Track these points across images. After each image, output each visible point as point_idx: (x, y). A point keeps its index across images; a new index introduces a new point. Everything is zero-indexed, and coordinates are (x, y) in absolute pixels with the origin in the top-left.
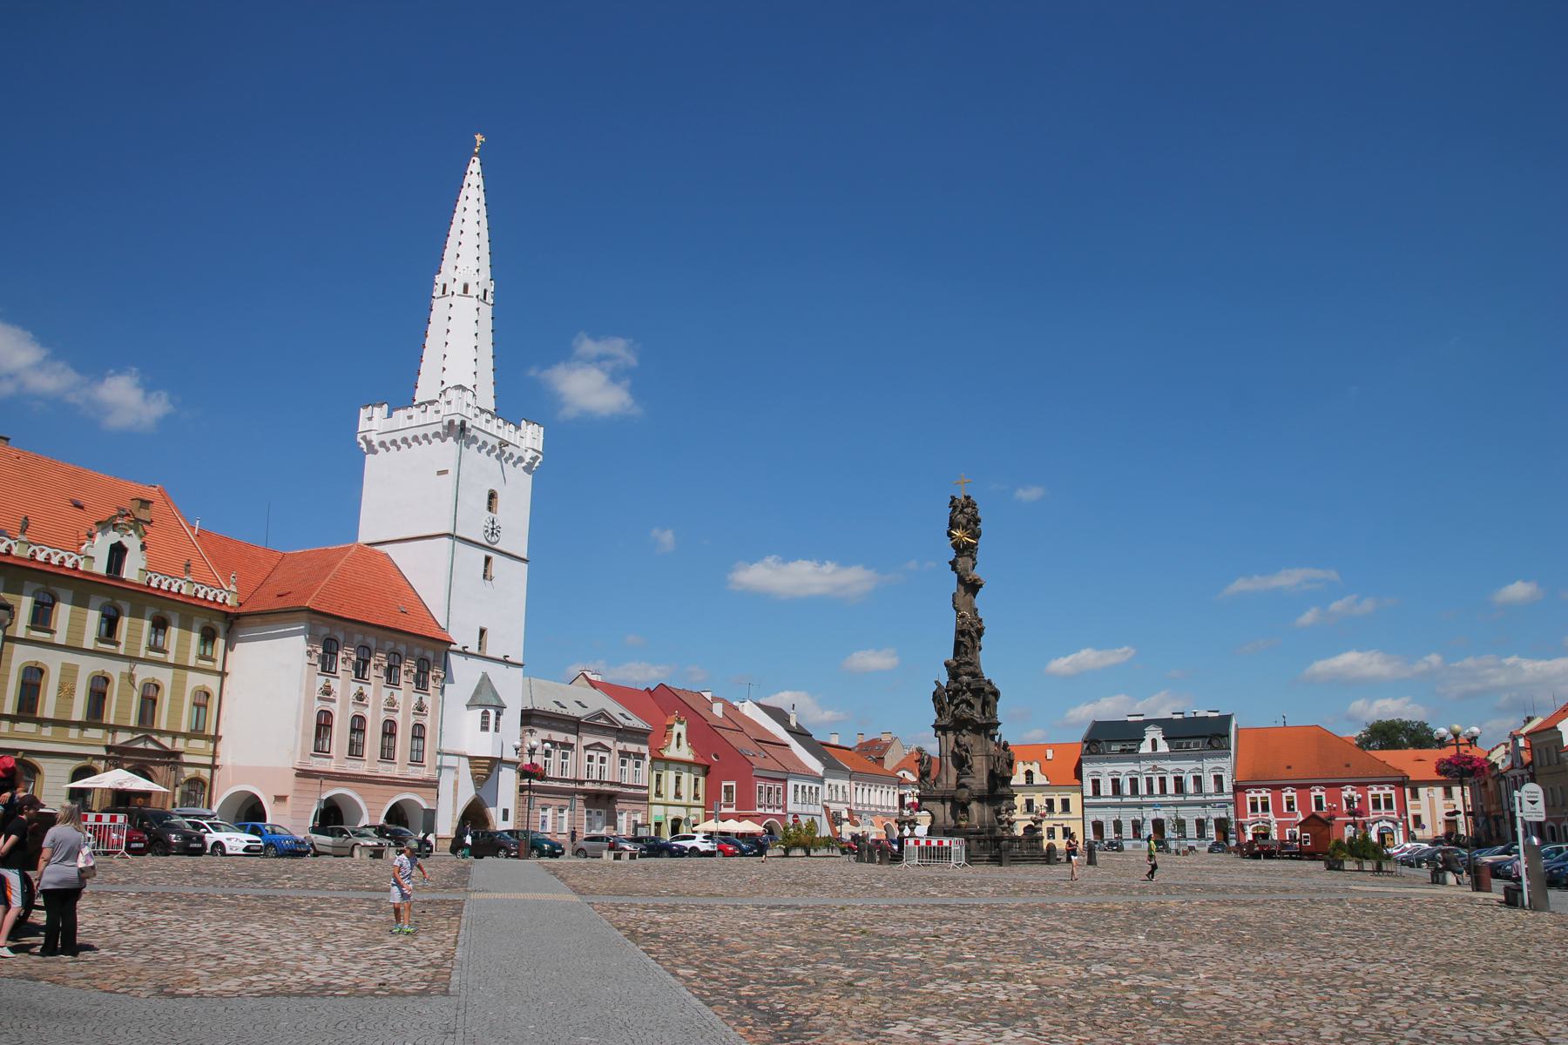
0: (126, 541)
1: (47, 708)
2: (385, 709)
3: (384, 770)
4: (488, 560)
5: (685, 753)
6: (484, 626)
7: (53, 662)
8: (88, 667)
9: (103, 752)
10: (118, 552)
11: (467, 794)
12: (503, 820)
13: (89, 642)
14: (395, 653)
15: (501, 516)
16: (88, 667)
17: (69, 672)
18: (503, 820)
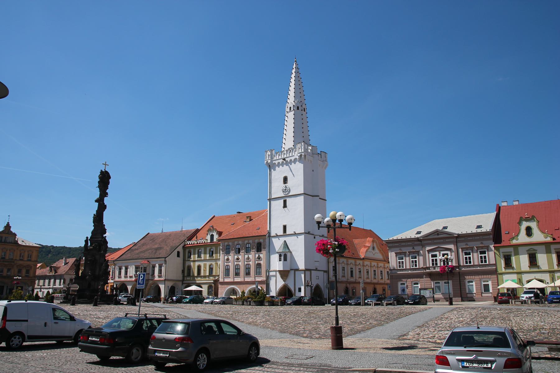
0: (213, 234)
1: (202, 274)
2: (246, 261)
3: (247, 279)
4: (285, 202)
5: (538, 236)
6: (285, 224)
7: (202, 264)
8: (208, 263)
9: (212, 281)
10: (212, 236)
11: (281, 283)
12: (299, 292)
13: (208, 258)
14: (238, 245)
15: (289, 184)
16: (208, 263)
17: (205, 265)
18: (299, 292)
